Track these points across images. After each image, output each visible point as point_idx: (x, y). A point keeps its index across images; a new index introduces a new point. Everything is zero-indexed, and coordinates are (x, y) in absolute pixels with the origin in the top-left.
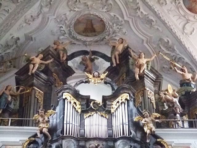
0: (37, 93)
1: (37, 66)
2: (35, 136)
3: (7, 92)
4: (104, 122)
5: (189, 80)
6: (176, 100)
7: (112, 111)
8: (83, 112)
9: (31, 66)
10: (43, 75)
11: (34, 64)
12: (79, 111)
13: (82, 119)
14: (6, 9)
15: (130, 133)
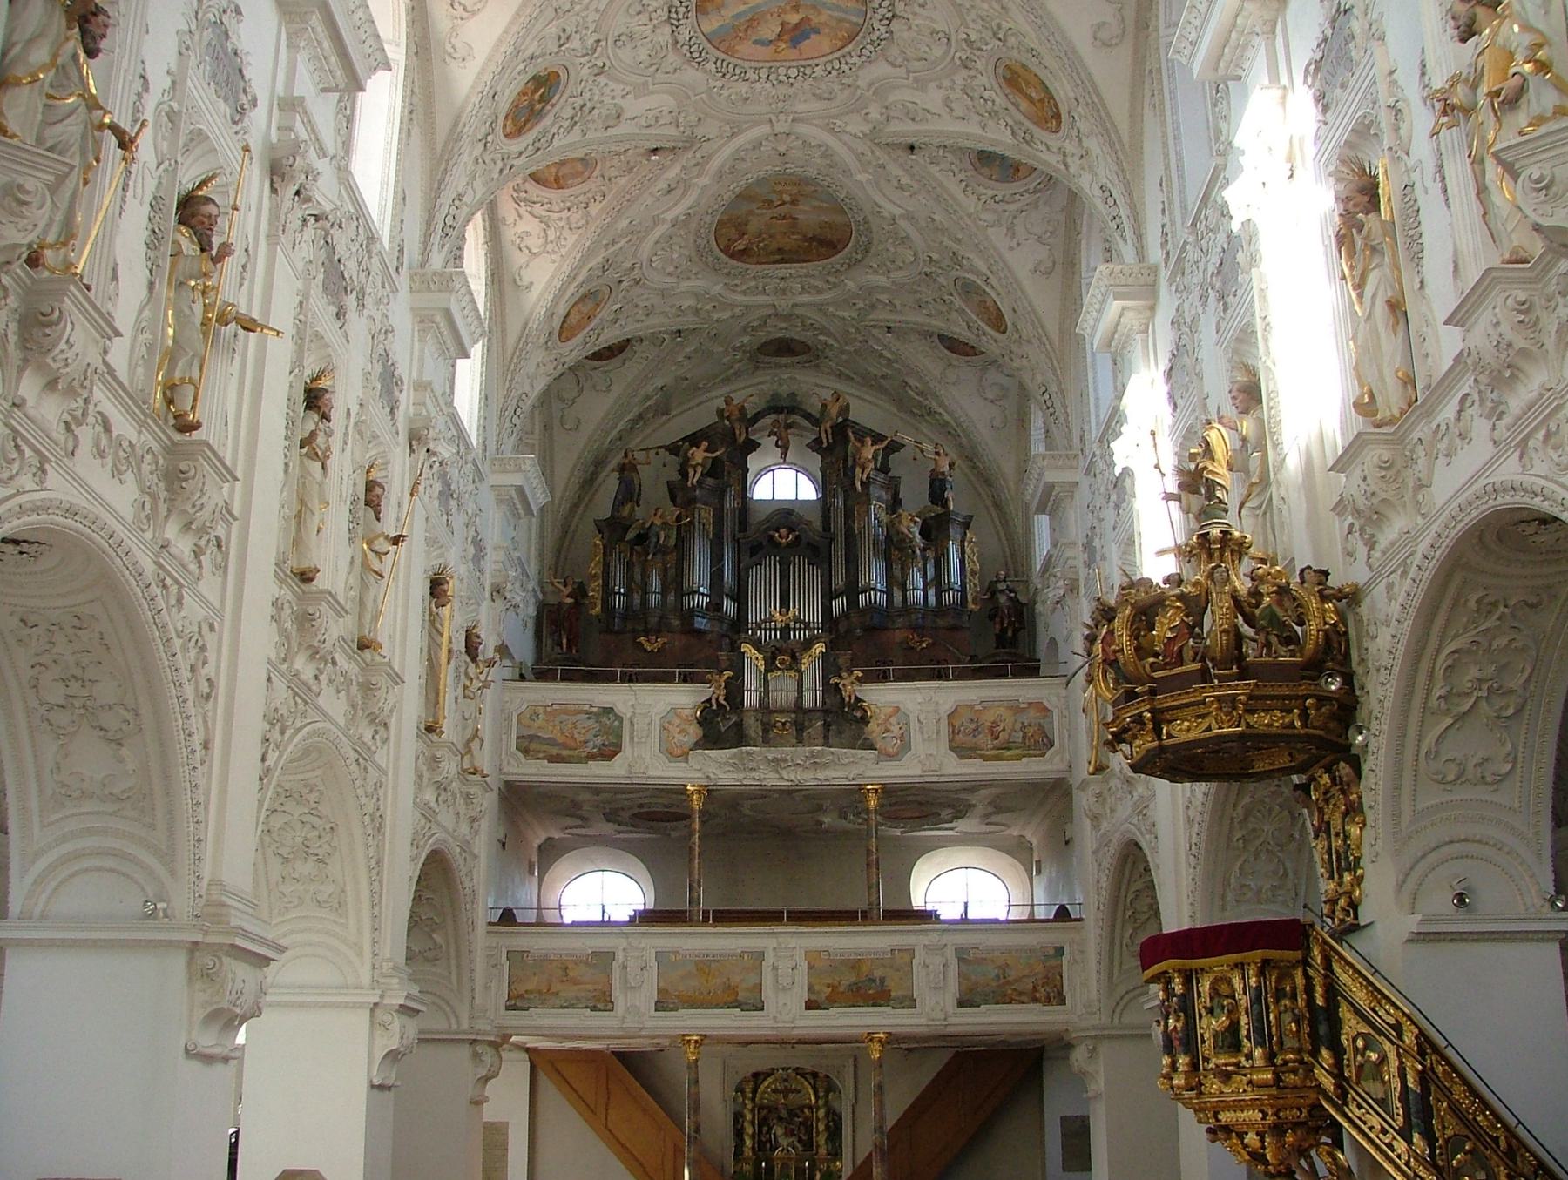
0: (702, 512)
1: (700, 470)
2: (709, 700)
3: (658, 522)
4: (793, 685)
5: (943, 473)
6: (916, 530)
7: (803, 668)
8: (767, 671)
9: (691, 473)
10: (710, 481)
11: (694, 467)
12: (763, 668)
13: (766, 680)
14: (644, 355)
15: (824, 702)
